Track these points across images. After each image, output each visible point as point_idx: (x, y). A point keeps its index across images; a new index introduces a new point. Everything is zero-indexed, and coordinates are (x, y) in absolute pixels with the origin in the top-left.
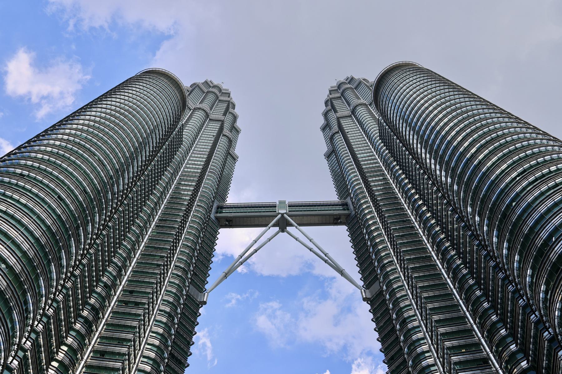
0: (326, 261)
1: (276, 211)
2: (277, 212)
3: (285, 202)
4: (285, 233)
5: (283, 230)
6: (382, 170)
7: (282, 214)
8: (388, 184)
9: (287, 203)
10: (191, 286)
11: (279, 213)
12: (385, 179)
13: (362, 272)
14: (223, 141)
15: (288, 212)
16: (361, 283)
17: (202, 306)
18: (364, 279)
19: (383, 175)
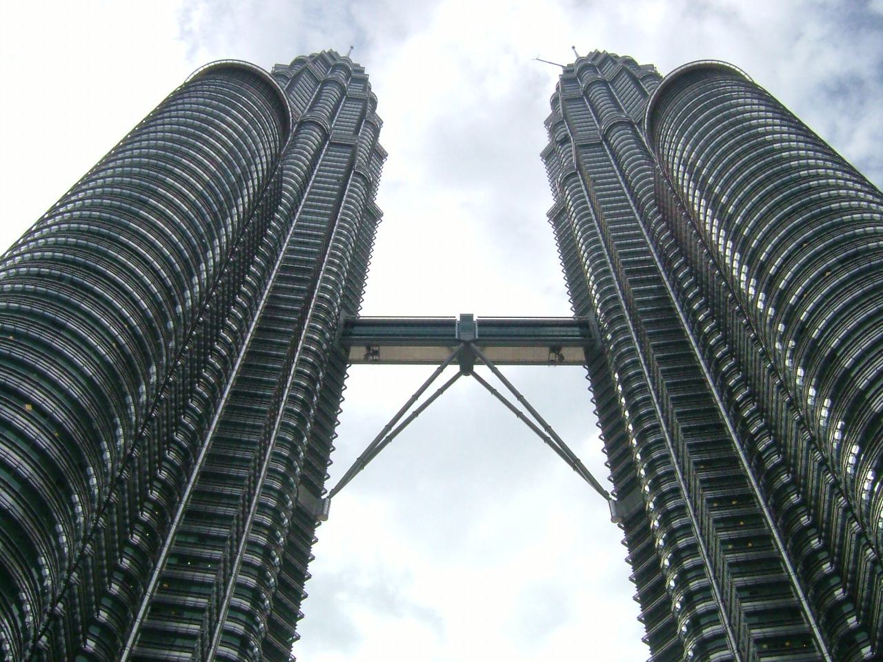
0: (546, 440)
1: (454, 335)
2: (457, 337)
3: (470, 317)
4: (471, 377)
5: (467, 370)
6: (655, 270)
7: (467, 344)
8: (667, 299)
9: (475, 319)
10: (302, 487)
11: (459, 341)
12: (663, 289)
13: (613, 464)
14: (354, 186)
15: (477, 337)
16: (609, 487)
17: (320, 524)
18: (616, 478)
19: (658, 280)
